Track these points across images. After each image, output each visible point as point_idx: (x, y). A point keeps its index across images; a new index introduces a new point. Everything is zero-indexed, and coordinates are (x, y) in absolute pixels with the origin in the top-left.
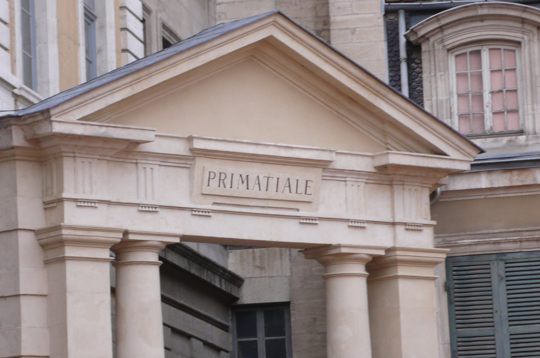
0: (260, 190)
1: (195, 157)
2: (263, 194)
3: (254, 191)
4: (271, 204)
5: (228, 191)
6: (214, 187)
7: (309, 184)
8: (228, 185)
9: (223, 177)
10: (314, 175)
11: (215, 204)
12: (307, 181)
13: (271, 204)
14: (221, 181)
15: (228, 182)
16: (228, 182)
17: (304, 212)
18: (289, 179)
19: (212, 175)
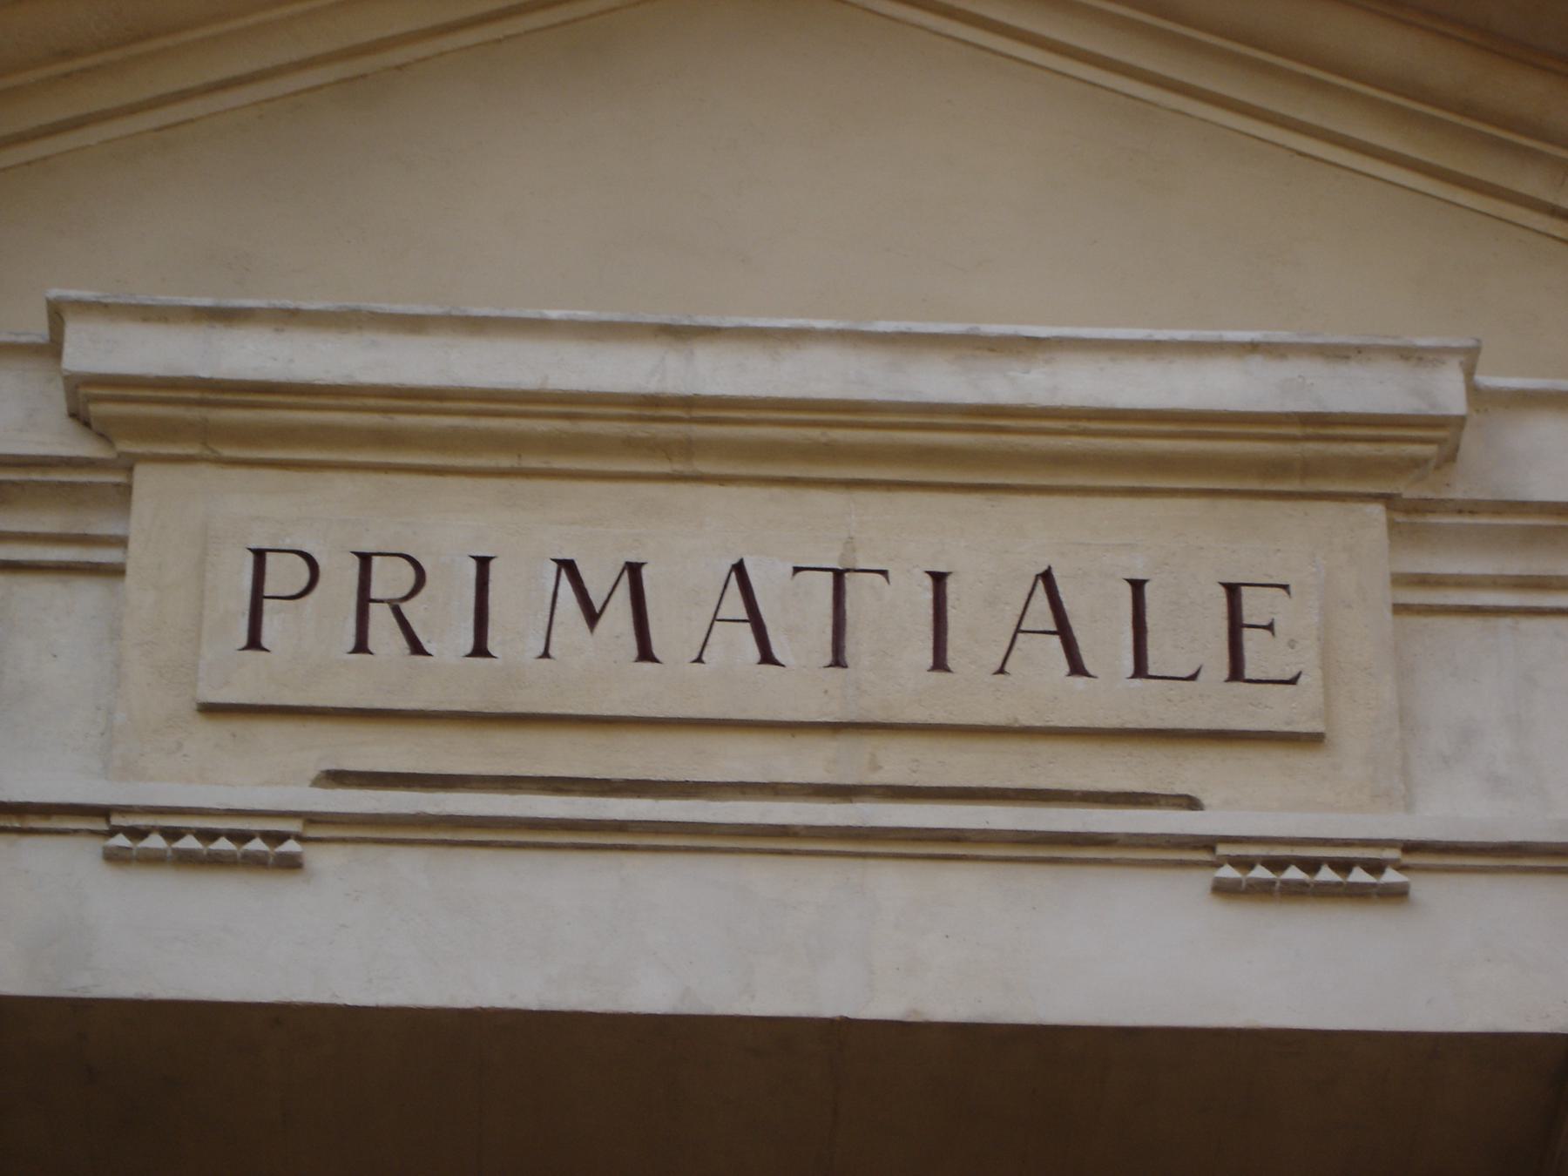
0: (767, 657)
1: (127, 465)
2: (802, 687)
3: (728, 676)
4: (897, 762)
5: (448, 676)
6: (309, 646)
7: (1254, 606)
8: (448, 632)
9: (390, 579)
10: (1324, 561)
11: (337, 778)
12: (1233, 591)
13: (897, 762)
14: (380, 616)
15: (444, 618)
16: (444, 618)
17: (1247, 802)
18: (1047, 577)
19: (284, 574)
